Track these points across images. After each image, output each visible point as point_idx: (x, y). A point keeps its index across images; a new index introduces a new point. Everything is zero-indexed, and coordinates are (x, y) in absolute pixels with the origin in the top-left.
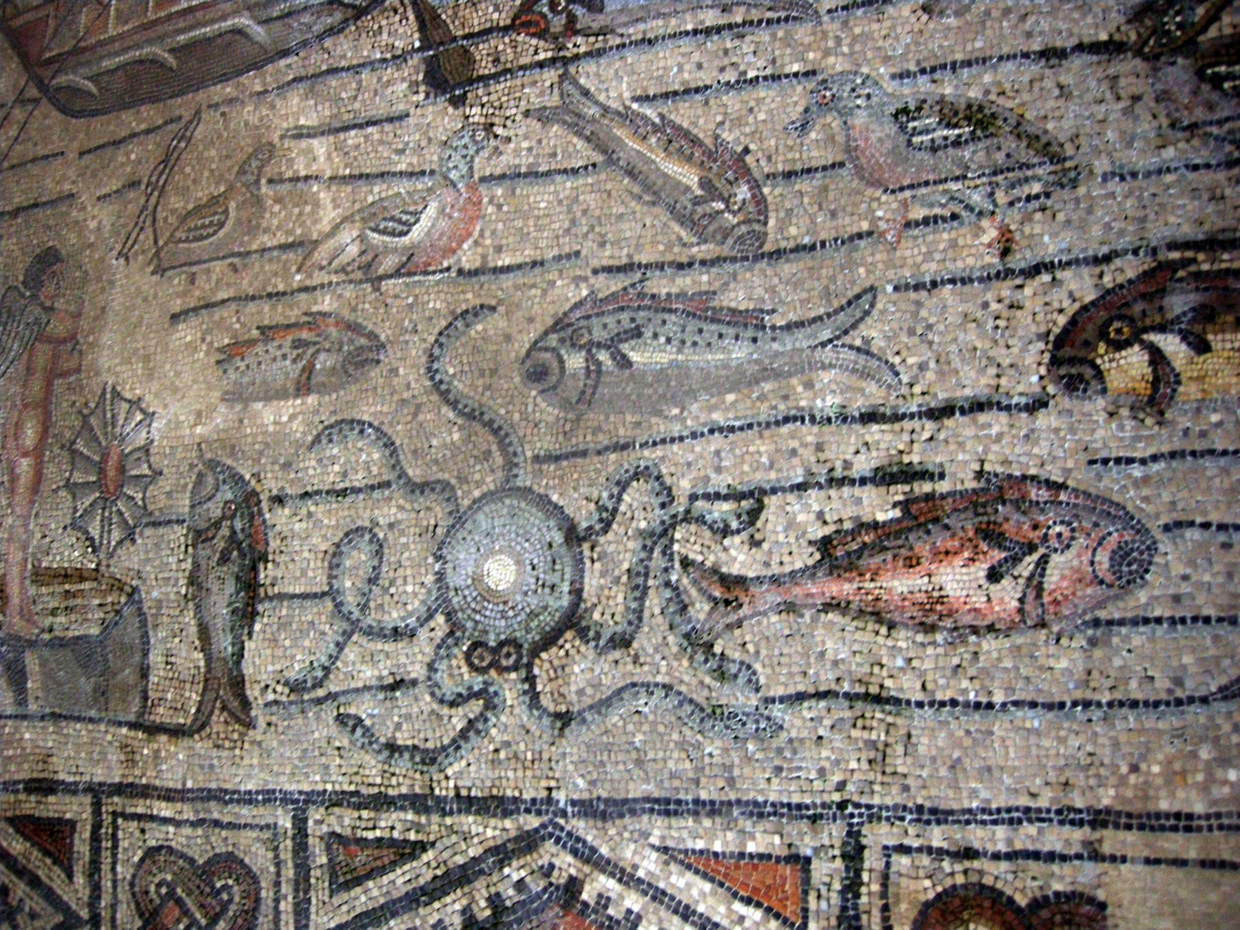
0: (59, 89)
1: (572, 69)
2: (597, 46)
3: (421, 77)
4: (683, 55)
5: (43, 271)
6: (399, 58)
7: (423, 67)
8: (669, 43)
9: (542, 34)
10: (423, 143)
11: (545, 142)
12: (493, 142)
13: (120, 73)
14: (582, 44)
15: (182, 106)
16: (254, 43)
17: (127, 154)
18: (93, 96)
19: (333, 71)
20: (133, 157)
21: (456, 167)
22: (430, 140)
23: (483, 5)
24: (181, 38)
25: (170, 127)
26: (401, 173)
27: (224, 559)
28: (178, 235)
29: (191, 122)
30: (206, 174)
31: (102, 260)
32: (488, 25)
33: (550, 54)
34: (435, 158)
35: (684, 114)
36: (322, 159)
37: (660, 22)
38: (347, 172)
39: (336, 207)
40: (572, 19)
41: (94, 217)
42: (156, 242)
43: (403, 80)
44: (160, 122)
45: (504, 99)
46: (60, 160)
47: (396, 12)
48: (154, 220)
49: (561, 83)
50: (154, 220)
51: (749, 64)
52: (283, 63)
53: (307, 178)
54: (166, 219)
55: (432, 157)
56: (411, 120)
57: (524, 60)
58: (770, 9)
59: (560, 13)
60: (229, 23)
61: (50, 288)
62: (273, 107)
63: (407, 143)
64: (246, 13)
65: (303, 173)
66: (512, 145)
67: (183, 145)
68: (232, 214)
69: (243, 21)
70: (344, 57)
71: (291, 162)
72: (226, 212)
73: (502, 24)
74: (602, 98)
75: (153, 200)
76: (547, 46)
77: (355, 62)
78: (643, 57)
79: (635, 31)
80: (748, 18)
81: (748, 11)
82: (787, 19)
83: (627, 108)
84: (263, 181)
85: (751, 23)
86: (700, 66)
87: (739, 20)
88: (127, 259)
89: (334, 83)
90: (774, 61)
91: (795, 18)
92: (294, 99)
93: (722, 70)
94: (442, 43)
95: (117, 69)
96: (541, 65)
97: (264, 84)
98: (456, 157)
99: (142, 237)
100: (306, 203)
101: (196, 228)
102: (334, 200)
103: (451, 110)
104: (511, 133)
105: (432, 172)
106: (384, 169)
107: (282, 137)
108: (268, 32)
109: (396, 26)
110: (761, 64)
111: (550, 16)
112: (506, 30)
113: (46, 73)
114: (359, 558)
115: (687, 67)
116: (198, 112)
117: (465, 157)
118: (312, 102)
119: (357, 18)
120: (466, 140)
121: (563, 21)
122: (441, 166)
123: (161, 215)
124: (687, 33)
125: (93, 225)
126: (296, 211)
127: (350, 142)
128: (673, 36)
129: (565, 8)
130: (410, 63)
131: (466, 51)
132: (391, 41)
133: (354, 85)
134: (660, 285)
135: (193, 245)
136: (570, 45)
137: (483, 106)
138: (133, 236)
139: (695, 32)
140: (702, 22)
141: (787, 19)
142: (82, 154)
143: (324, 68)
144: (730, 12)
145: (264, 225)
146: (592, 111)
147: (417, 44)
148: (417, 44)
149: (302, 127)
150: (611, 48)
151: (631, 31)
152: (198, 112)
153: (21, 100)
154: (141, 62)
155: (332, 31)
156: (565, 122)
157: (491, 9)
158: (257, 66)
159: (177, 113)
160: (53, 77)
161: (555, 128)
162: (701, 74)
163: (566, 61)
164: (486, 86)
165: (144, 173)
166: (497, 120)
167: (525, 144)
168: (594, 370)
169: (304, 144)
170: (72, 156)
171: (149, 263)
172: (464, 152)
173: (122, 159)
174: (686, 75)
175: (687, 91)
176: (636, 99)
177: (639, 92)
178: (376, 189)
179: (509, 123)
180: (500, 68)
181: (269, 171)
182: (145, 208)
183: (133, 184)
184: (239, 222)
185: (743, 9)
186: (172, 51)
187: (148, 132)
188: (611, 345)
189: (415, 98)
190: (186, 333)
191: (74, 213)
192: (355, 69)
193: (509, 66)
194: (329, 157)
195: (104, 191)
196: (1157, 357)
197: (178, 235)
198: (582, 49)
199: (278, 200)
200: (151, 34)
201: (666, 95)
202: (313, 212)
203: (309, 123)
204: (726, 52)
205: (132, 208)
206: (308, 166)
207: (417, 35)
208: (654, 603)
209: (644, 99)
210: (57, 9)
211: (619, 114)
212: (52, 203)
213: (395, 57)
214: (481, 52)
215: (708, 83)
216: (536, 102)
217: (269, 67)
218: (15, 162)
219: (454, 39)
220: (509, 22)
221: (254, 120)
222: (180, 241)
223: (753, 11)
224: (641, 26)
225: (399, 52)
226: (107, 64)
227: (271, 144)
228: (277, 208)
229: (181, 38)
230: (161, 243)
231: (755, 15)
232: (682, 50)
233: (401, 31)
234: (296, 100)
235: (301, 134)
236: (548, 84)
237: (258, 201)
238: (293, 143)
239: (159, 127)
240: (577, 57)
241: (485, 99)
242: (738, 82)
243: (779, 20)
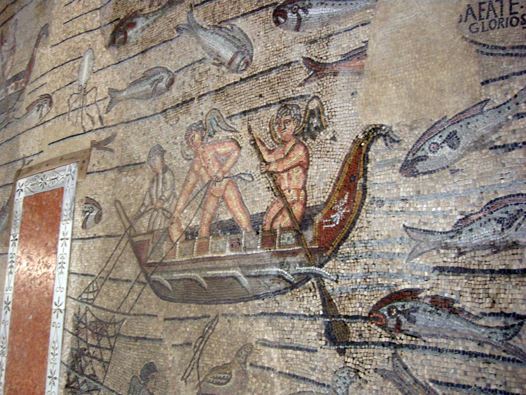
0: (155, 281)
1: (399, 352)
2: (412, 343)
3: (323, 332)
4: (457, 364)
5: (149, 373)
6: (313, 317)
7: (324, 327)
8: (450, 355)
9: (383, 327)
10: (324, 369)
11: (384, 389)
12: (358, 380)
13: (181, 282)
14: (402, 339)
15: (211, 310)
16: (243, 287)
17: (185, 327)
18: (169, 290)
19: (281, 314)
20: (188, 329)
21: (340, 387)
22: (327, 368)
23: (354, 301)
24: (209, 273)
25: (205, 320)
26: (313, 381)
28: (209, 378)
29: (214, 320)
30: (221, 351)
31: (174, 378)
32: (356, 314)
33: (387, 340)
34: (330, 379)
36: (275, 360)
37: (445, 341)
38: (288, 371)
39: (282, 389)
40: (399, 323)
41: (171, 355)
42: (199, 378)
43: (315, 330)
44: (200, 315)
45: (364, 358)
46: (155, 319)
47: (311, 290)
48: (198, 367)
49: (393, 358)
50: (198, 367)
51: (492, 380)
52: (257, 302)
53: (268, 369)
54: (203, 367)
55: (329, 379)
56: (318, 354)
57: (375, 339)
58: (504, 351)
59: (393, 317)
60: (231, 272)
61: (151, 384)
62: (252, 325)
63: (316, 366)
64: (239, 268)
65: (266, 365)
66: (368, 386)
67: (210, 331)
68: (234, 376)
69: (237, 272)
70: (285, 307)
71: (261, 357)
72: (230, 374)
73: (363, 315)
74: (414, 373)
75: (197, 355)
76: (386, 334)
77: (291, 312)
78: (436, 358)
79: (432, 342)
80: (492, 353)
81: (492, 349)
82: (513, 360)
83: (427, 384)
84: (248, 364)
85: (494, 356)
86: (465, 373)
87: (487, 352)
88: (186, 382)
89: (281, 321)
90: (505, 383)
91: (518, 361)
92: (262, 324)
93: (477, 379)
94: (333, 316)
95: (180, 280)
96: (383, 344)
97: (248, 311)
98: (340, 382)
99: (192, 373)
100: (268, 382)
101: (217, 378)
102: (281, 385)
103: (338, 355)
104: (368, 379)
105: (328, 386)
106: (306, 376)
107: (257, 343)
108: (249, 281)
109: (311, 298)
110: (498, 382)
111: (388, 317)
112: (365, 319)
113: (150, 270)
115: (459, 371)
116: (217, 316)
117: (345, 383)
118: (270, 328)
119: (292, 288)
120: (345, 375)
121: (395, 323)
122: (333, 385)
123: (201, 365)
124: (459, 352)
125: (170, 358)
126: (263, 384)
127: (289, 355)
128: (452, 351)
129: (396, 315)
130: (318, 322)
131: (346, 325)
132: (308, 306)
133: (290, 325)
135: (216, 386)
136: (398, 338)
137: (354, 358)
138: (188, 371)
139: (464, 353)
140: (467, 348)
141: (513, 360)
142: (165, 319)
143: (276, 311)
144: (483, 346)
145: (249, 387)
146: (408, 379)
147: (321, 313)
148: (321, 313)
149: (266, 340)
150: (419, 347)
151: (430, 340)
152: (217, 316)
153: (138, 281)
154: (191, 280)
155: (279, 292)
156: (394, 382)
157: (358, 305)
158: (245, 300)
159: (208, 313)
160: (152, 275)
161: (390, 383)
162: (466, 378)
163: (397, 347)
164: (355, 348)
165: (194, 339)
166: (360, 369)
167: (374, 387)
169: (267, 349)
170: (161, 319)
171: (196, 388)
172: (344, 381)
173: (183, 329)
174: (458, 377)
175: (458, 386)
176: (432, 381)
177: (433, 377)
178: (301, 385)
179: (366, 372)
180: (362, 340)
181: (251, 359)
182: (193, 359)
183: (189, 344)
184: (236, 382)
185: (489, 347)
186: (205, 278)
187: (195, 318)
189: (320, 342)
191: (162, 349)
192: (292, 316)
193: (367, 340)
194: (279, 361)
195: (175, 343)
197: (209, 378)
198: (404, 342)
199: (255, 376)
200: (195, 266)
201: (447, 384)
202: (271, 388)
203: (269, 339)
204: (480, 369)
205: (188, 356)
206: (269, 362)
207: (321, 307)
209: (436, 382)
210: (153, 238)
211: (422, 385)
212: (153, 340)
213: (311, 316)
214: (354, 327)
215: (470, 384)
216: (380, 366)
217: (250, 303)
218: (136, 312)
219: (339, 316)
220: (367, 315)
221: (243, 329)
222: (209, 382)
223: (495, 350)
224: (435, 340)
225: (312, 314)
226: (176, 276)
227: (251, 344)
228: (254, 380)
229: (209, 273)
230: (201, 379)
231: (496, 352)
232: (457, 361)
233: (313, 302)
234: (263, 325)
235: (265, 344)
236: (386, 356)
237: (245, 373)
238: (262, 348)
239: (200, 318)
240: (401, 346)
241: (355, 355)
242: (486, 389)
243: (509, 360)
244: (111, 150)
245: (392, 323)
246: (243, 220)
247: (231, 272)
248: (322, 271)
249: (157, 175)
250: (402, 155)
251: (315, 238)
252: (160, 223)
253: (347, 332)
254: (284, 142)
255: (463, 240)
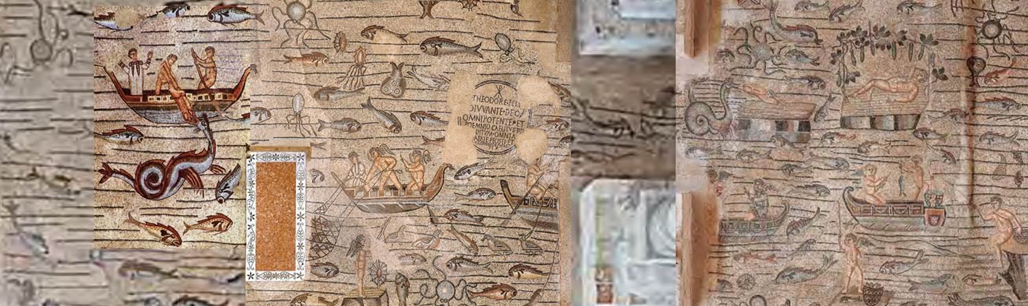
14: (453, 222)
27: (402, 287)
35: (468, 235)
92: (408, 219)
114: (424, 287)
134: (465, 257)
168: (456, 266)
188: (458, 263)
190: (392, 253)
196: (519, 273)
208: (465, 294)
244: (325, 149)
245: (451, 218)
246: (399, 186)
247: (395, 203)
248: (429, 203)
249: (355, 164)
250: (455, 173)
251: (427, 194)
252: (359, 183)
253: (438, 221)
254: (415, 163)
255: (471, 198)
